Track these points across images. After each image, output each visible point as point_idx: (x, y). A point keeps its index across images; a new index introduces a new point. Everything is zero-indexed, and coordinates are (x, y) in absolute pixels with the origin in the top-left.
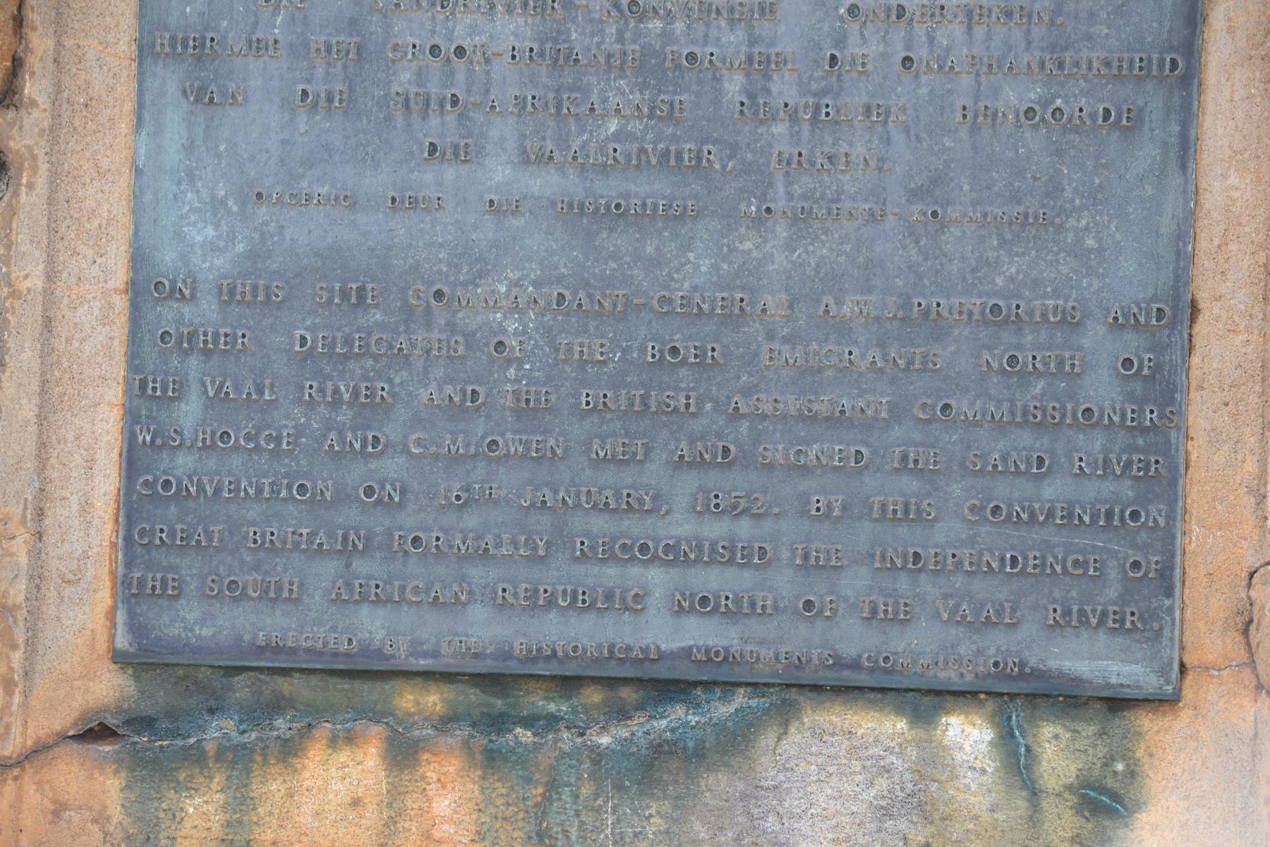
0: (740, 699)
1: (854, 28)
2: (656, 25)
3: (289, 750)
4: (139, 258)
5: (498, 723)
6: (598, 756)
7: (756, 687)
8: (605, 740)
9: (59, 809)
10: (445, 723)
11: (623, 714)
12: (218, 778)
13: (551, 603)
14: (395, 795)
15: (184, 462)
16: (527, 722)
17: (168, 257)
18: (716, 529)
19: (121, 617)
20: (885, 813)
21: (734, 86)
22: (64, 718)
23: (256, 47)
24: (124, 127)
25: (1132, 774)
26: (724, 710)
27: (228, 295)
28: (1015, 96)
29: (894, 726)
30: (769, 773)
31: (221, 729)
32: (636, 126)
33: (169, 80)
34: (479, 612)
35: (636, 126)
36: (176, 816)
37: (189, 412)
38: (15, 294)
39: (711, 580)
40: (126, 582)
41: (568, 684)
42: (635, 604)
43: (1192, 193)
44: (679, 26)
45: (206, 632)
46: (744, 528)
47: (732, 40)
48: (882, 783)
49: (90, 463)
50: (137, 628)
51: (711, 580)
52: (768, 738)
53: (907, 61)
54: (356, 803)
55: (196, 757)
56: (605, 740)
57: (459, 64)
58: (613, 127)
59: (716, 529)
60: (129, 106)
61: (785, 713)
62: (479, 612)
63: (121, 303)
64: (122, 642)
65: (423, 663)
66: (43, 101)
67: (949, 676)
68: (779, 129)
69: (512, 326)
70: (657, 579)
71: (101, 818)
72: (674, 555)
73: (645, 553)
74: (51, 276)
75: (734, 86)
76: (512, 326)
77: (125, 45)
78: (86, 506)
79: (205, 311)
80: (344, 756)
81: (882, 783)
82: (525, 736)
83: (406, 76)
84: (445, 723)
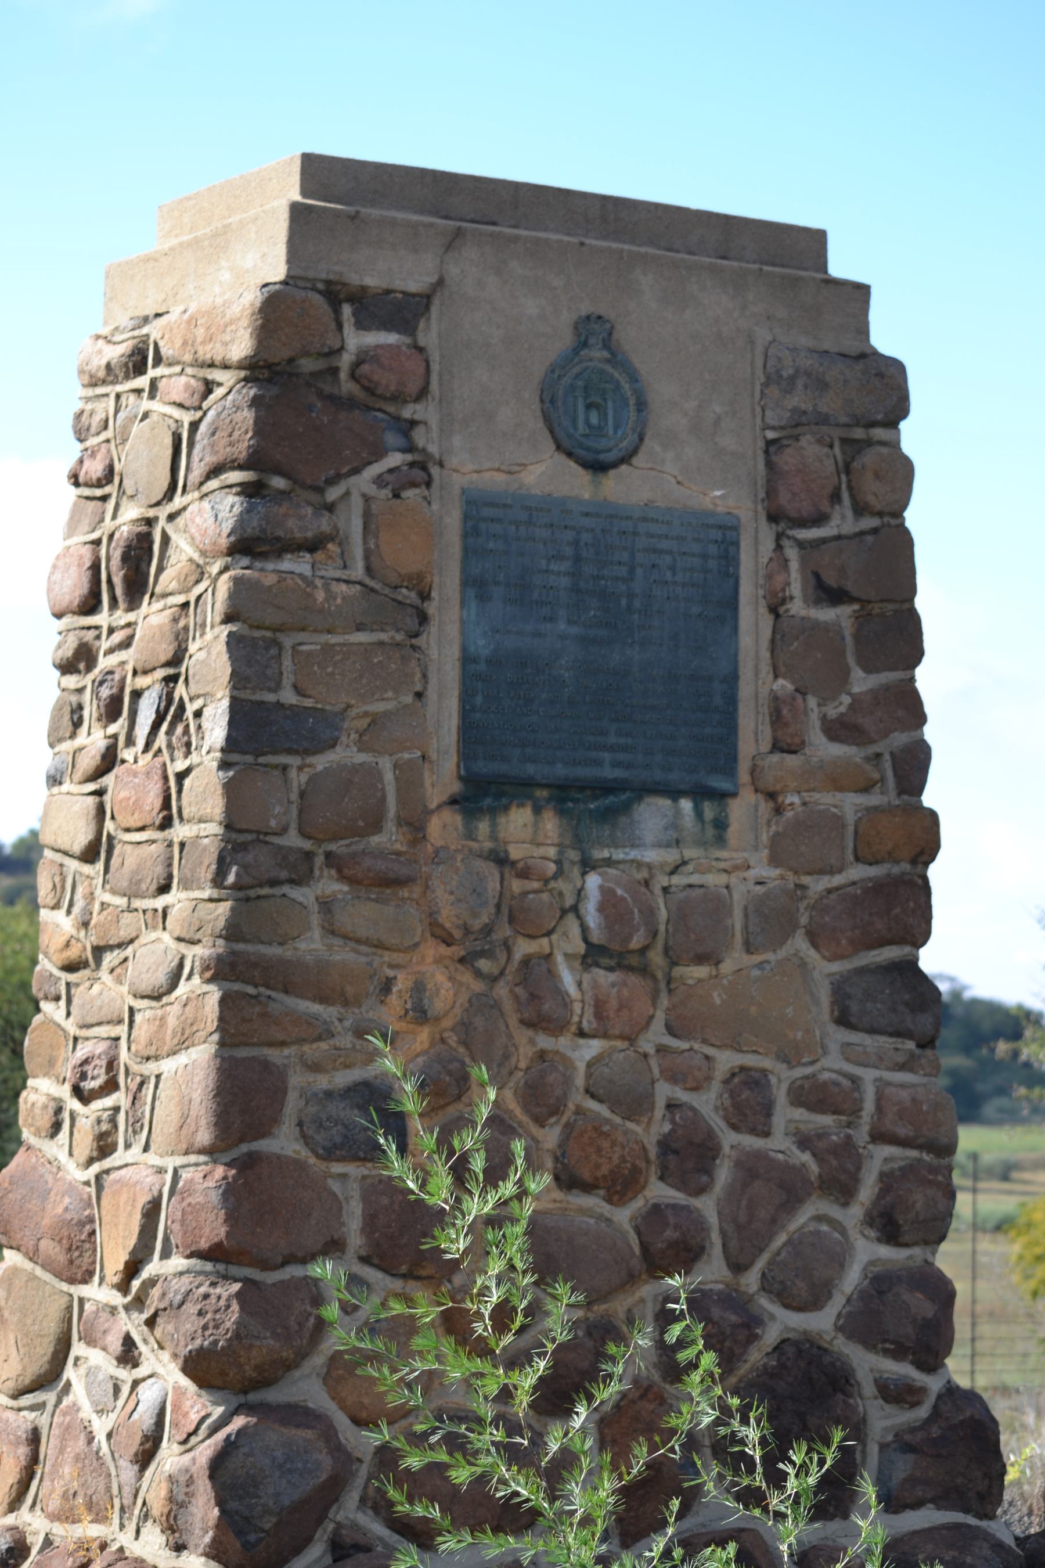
0: (628, 794)
1: (654, 586)
2: (603, 582)
3: (506, 809)
4: (464, 649)
5: (563, 800)
6: (590, 811)
7: (633, 790)
8: (592, 806)
9: (445, 826)
10: (549, 800)
11: (596, 798)
12: (487, 818)
13: (580, 763)
14: (536, 824)
15: (478, 715)
16: (572, 800)
17: (472, 649)
18: (622, 741)
19: (462, 765)
20: (666, 828)
21: (624, 602)
22: (444, 797)
23: (497, 583)
24: (457, 607)
25: (726, 817)
26: (624, 797)
27: (488, 662)
28: (695, 610)
29: (668, 802)
30: (636, 817)
31: (488, 801)
32: (598, 613)
33: (471, 593)
34: (559, 765)
35: (598, 613)
36: (477, 828)
37: (479, 700)
38: (430, 660)
39: (621, 756)
40: (464, 754)
41: (582, 789)
42: (598, 763)
43: (737, 642)
44: (609, 583)
45: (485, 770)
46: (629, 741)
47: (624, 587)
48: (665, 820)
49: (450, 716)
50: (466, 769)
51: (621, 756)
52: (635, 806)
53: (668, 598)
54: (525, 825)
55: (481, 810)
56: (592, 806)
57: (551, 592)
58: (592, 613)
59: (622, 741)
60: (458, 601)
61: (640, 799)
62: (559, 765)
63: (457, 664)
64: (462, 773)
65: (545, 781)
66: (437, 598)
67: (682, 787)
68: (636, 616)
69: (567, 675)
70: (607, 756)
71: (456, 829)
72: (612, 749)
73: (604, 748)
74: (439, 654)
75: (624, 602)
76: (567, 675)
77: (457, 582)
78: (449, 729)
79: (482, 667)
80: (521, 810)
81: (665, 820)
82: (570, 805)
83: (536, 594)
84: (549, 800)
